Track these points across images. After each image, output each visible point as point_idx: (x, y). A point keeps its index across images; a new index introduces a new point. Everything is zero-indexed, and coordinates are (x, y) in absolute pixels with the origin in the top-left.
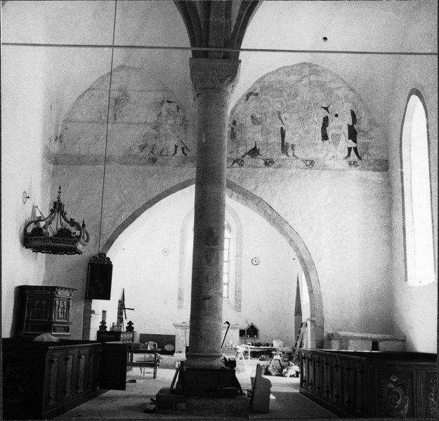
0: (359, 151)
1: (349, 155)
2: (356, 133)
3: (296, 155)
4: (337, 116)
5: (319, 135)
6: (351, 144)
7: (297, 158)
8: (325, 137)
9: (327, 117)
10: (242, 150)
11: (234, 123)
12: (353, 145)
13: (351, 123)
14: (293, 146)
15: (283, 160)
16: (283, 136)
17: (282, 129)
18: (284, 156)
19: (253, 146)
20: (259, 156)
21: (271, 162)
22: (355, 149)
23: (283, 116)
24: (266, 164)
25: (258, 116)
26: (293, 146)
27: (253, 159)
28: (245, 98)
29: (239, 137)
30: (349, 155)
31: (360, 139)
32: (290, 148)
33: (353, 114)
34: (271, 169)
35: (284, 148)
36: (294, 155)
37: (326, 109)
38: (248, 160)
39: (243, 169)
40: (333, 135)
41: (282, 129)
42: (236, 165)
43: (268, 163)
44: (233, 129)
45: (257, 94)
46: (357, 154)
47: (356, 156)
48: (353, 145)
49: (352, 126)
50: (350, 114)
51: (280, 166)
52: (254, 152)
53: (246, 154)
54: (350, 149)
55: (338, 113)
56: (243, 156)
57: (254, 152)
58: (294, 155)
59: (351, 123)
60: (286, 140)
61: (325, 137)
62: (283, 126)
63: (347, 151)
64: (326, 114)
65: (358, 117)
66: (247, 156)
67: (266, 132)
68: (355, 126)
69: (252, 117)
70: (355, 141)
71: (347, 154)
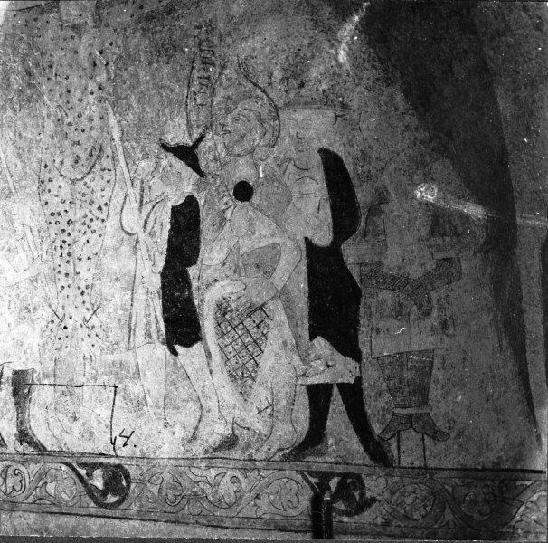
2: (356, 295)
4: (243, 192)
5: (150, 309)
6: (326, 364)
9: (191, 202)
13: (323, 238)
22: (353, 393)
31: (385, 337)
37: (187, 154)
40: (222, 309)
47: (355, 444)
49: (334, 251)
50: (319, 175)
54: (319, 396)
59: (323, 238)
63: (303, 400)
64: (184, 184)
65: (363, 195)
68: (352, 253)
70: (347, 345)
71: (303, 427)
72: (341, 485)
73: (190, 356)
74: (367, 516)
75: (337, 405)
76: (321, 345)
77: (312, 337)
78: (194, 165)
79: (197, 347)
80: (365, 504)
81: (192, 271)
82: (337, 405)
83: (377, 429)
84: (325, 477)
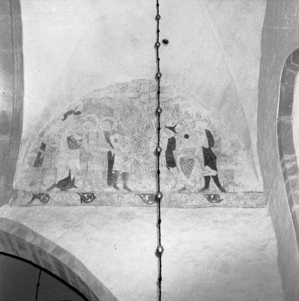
0: (221, 181)
1: (207, 186)
3: (130, 186)
4: (187, 136)
7: (130, 190)
8: (171, 163)
10: (50, 180)
11: (43, 146)
12: (213, 173)
13: (207, 146)
14: (125, 176)
15: (108, 195)
16: (111, 162)
17: (110, 153)
18: (111, 189)
19: (66, 176)
20: (73, 189)
21: (90, 197)
22: (216, 179)
23: (112, 138)
24: (83, 200)
25: (78, 138)
26: (125, 176)
27: (63, 193)
28: (63, 117)
29: (45, 164)
30: (207, 186)
32: (120, 177)
33: (209, 134)
34: (88, 208)
35: (111, 177)
36: (125, 187)
38: (56, 195)
39: (46, 207)
40: (182, 159)
41: (110, 153)
42: (37, 201)
43: (88, 198)
44: (39, 154)
45: (79, 113)
46: (218, 185)
47: (217, 188)
48: (213, 173)
49: (209, 149)
50: (205, 135)
51: (102, 203)
52: (66, 183)
53: (54, 186)
54: (207, 179)
55: (188, 133)
56: (48, 190)
57: (66, 183)
58: (125, 187)
59: (207, 146)
60: (116, 167)
61: (171, 163)
62: (113, 152)
63: (204, 179)
64: (172, 134)
65: (216, 139)
66: (56, 189)
67: (85, 158)
68: (213, 150)
69: (69, 139)
71: (203, 185)
72: (214, 197)
73: (173, 170)
74: (221, 203)
75: (212, 180)
76: (207, 167)
77: (205, 165)
78: (174, 131)
79: (175, 168)
80: (220, 201)
81: (174, 152)
82: (212, 180)
83: (222, 185)
84: (210, 196)
